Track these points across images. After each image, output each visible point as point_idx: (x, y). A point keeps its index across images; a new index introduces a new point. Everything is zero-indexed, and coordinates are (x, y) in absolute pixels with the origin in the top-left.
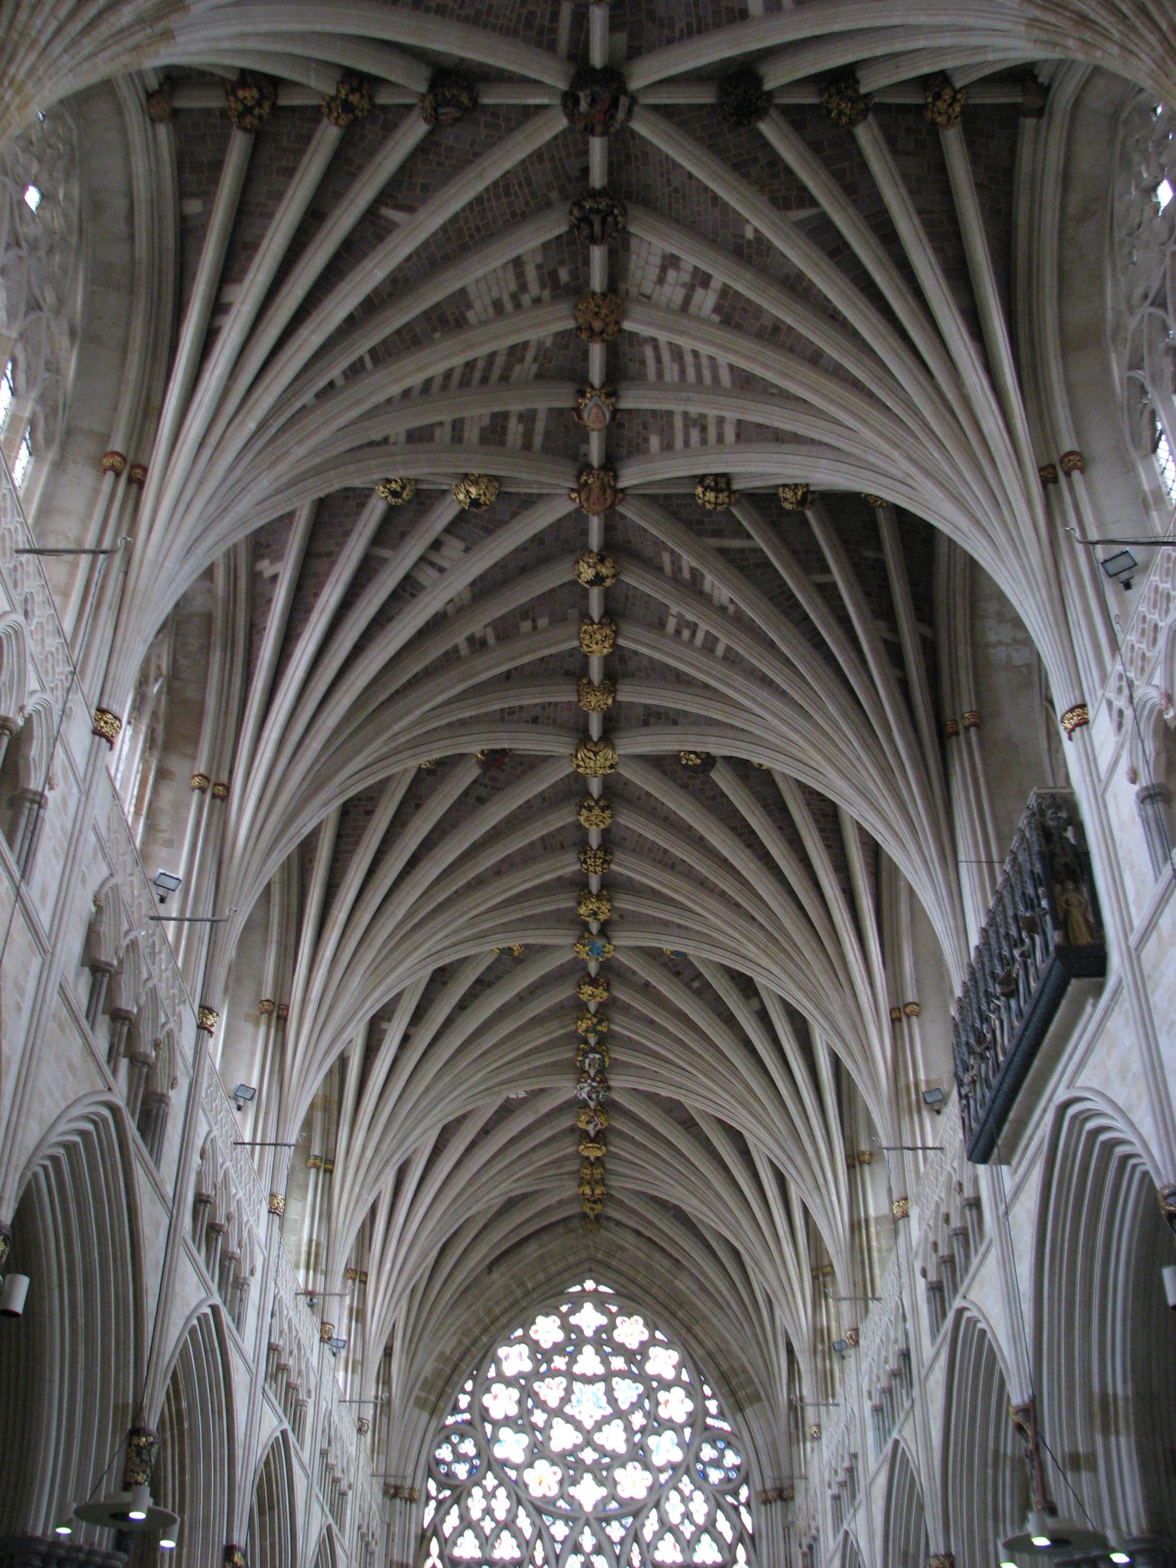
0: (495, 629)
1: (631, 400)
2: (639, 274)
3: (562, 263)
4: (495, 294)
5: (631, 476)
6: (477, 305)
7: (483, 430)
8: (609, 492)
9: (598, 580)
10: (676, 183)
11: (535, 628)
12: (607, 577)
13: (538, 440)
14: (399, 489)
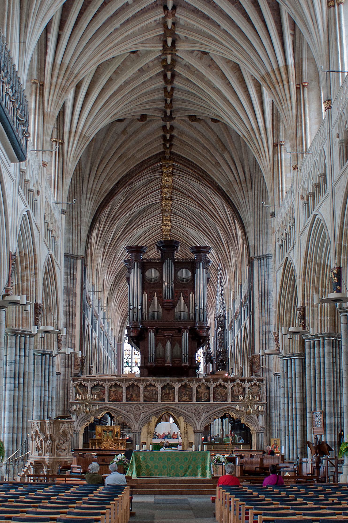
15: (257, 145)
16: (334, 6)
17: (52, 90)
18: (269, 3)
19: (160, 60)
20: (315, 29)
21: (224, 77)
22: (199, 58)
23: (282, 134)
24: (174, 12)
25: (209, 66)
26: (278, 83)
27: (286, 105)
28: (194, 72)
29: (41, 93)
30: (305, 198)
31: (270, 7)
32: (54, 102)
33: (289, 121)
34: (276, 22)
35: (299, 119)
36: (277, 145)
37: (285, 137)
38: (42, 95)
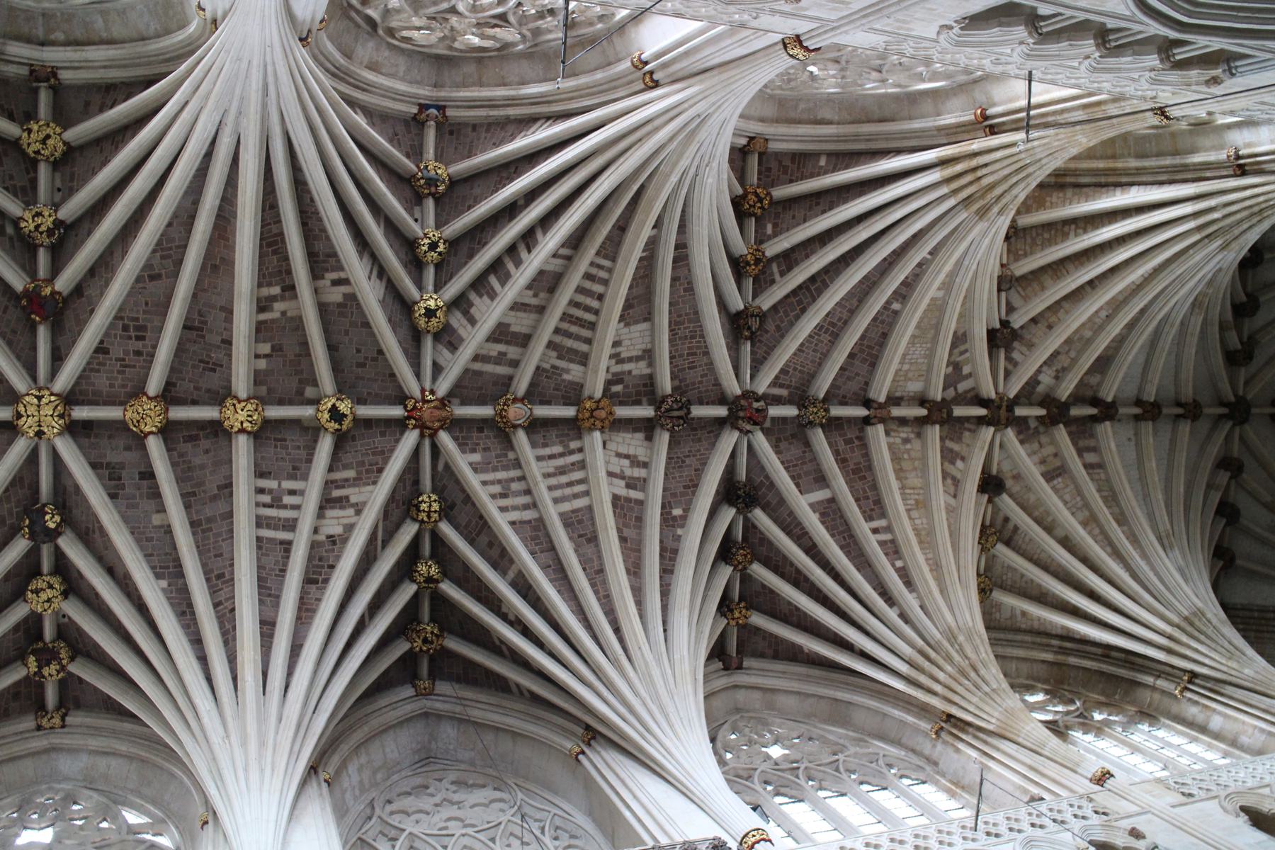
0: (273, 321)
1: (521, 438)
2: (620, 440)
3: (625, 387)
4: (626, 343)
5: (445, 438)
6: (626, 330)
7: (509, 325)
8: (437, 424)
9: (335, 414)
10: (688, 461)
11: (257, 356)
12: (341, 424)
13: (477, 366)
14: (438, 250)
15: (1238, 216)
16: (651, 73)
17: (956, 699)
18: (824, 212)
19: (1042, 429)
20: (686, 110)
21: (1076, 295)
22: (1028, 350)
23: (1212, 157)
24: (875, 405)
25: (1050, 327)
26: (980, 178)
27: (1023, 156)
28: (1072, 359)
29: (962, 725)
30: (1214, 73)
31: (831, 209)
32: (981, 705)
33: (1056, 143)
34: (861, 194)
35: (1050, 119)
36: (1240, 166)
37: (1221, 147)
38: (964, 725)
